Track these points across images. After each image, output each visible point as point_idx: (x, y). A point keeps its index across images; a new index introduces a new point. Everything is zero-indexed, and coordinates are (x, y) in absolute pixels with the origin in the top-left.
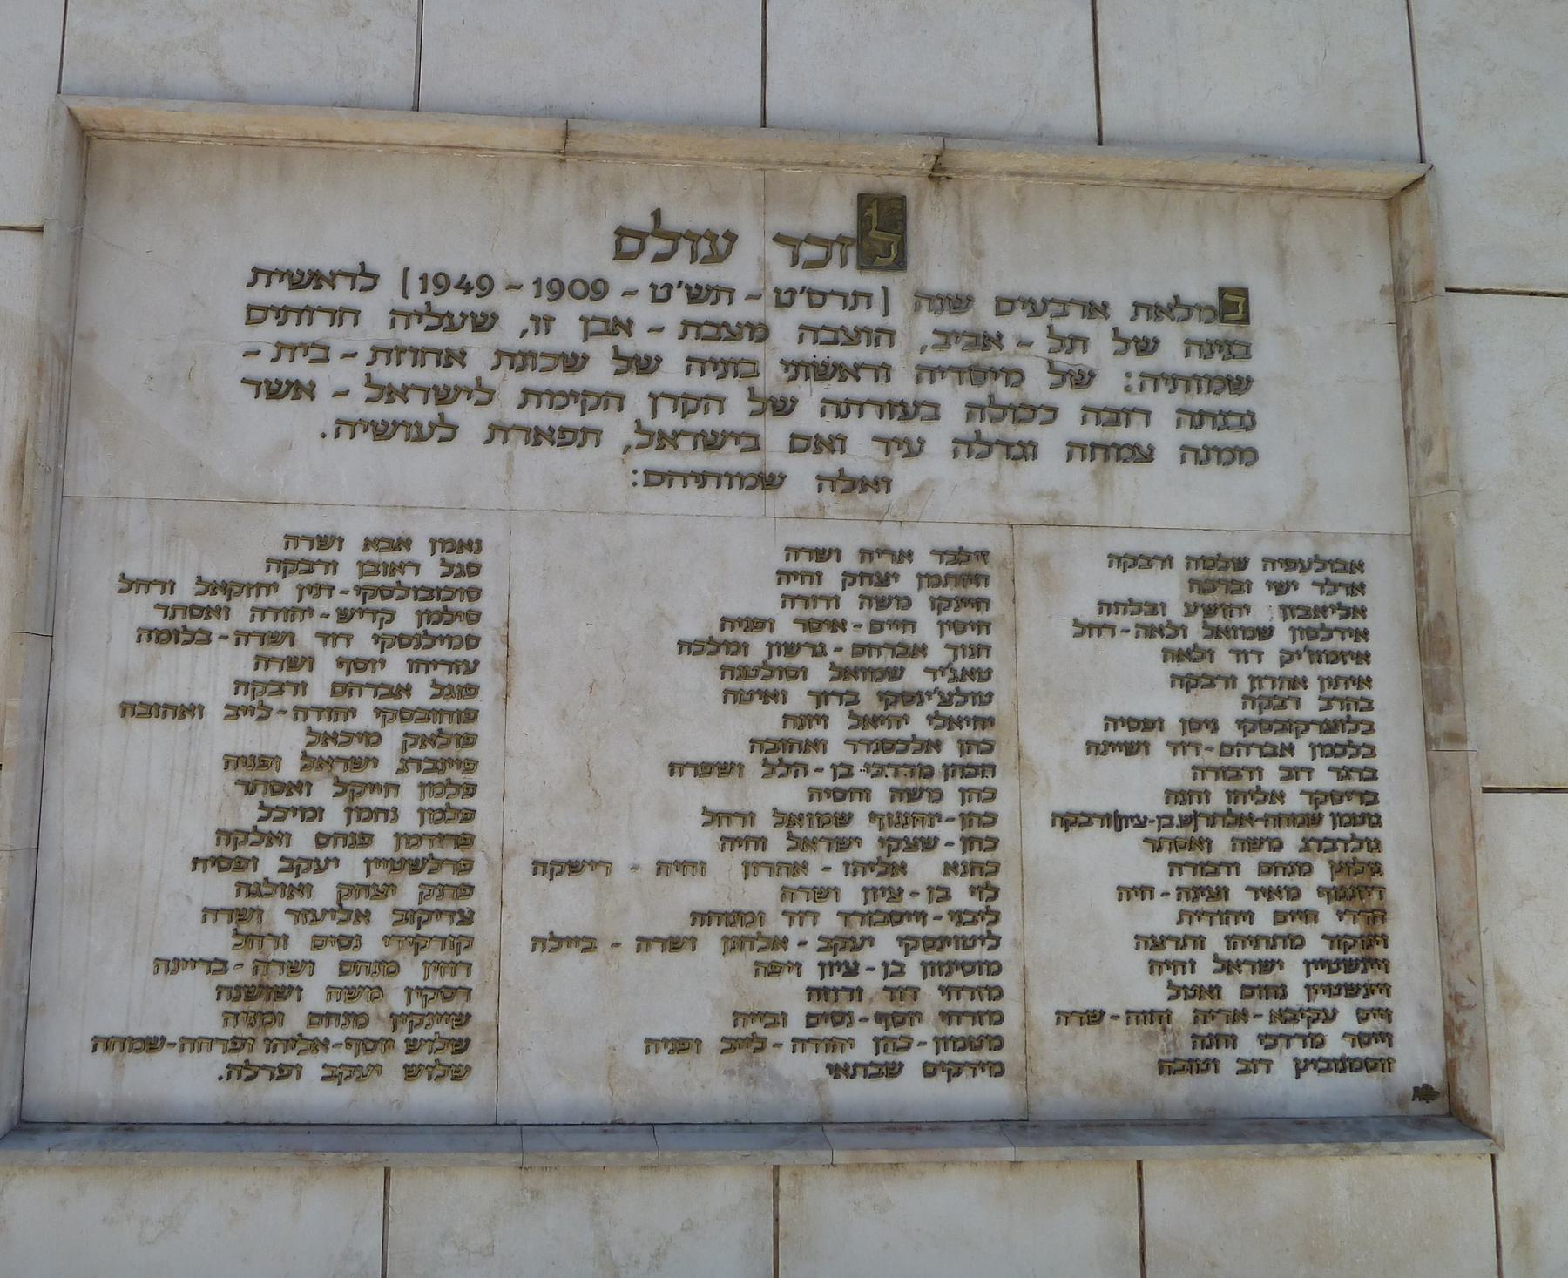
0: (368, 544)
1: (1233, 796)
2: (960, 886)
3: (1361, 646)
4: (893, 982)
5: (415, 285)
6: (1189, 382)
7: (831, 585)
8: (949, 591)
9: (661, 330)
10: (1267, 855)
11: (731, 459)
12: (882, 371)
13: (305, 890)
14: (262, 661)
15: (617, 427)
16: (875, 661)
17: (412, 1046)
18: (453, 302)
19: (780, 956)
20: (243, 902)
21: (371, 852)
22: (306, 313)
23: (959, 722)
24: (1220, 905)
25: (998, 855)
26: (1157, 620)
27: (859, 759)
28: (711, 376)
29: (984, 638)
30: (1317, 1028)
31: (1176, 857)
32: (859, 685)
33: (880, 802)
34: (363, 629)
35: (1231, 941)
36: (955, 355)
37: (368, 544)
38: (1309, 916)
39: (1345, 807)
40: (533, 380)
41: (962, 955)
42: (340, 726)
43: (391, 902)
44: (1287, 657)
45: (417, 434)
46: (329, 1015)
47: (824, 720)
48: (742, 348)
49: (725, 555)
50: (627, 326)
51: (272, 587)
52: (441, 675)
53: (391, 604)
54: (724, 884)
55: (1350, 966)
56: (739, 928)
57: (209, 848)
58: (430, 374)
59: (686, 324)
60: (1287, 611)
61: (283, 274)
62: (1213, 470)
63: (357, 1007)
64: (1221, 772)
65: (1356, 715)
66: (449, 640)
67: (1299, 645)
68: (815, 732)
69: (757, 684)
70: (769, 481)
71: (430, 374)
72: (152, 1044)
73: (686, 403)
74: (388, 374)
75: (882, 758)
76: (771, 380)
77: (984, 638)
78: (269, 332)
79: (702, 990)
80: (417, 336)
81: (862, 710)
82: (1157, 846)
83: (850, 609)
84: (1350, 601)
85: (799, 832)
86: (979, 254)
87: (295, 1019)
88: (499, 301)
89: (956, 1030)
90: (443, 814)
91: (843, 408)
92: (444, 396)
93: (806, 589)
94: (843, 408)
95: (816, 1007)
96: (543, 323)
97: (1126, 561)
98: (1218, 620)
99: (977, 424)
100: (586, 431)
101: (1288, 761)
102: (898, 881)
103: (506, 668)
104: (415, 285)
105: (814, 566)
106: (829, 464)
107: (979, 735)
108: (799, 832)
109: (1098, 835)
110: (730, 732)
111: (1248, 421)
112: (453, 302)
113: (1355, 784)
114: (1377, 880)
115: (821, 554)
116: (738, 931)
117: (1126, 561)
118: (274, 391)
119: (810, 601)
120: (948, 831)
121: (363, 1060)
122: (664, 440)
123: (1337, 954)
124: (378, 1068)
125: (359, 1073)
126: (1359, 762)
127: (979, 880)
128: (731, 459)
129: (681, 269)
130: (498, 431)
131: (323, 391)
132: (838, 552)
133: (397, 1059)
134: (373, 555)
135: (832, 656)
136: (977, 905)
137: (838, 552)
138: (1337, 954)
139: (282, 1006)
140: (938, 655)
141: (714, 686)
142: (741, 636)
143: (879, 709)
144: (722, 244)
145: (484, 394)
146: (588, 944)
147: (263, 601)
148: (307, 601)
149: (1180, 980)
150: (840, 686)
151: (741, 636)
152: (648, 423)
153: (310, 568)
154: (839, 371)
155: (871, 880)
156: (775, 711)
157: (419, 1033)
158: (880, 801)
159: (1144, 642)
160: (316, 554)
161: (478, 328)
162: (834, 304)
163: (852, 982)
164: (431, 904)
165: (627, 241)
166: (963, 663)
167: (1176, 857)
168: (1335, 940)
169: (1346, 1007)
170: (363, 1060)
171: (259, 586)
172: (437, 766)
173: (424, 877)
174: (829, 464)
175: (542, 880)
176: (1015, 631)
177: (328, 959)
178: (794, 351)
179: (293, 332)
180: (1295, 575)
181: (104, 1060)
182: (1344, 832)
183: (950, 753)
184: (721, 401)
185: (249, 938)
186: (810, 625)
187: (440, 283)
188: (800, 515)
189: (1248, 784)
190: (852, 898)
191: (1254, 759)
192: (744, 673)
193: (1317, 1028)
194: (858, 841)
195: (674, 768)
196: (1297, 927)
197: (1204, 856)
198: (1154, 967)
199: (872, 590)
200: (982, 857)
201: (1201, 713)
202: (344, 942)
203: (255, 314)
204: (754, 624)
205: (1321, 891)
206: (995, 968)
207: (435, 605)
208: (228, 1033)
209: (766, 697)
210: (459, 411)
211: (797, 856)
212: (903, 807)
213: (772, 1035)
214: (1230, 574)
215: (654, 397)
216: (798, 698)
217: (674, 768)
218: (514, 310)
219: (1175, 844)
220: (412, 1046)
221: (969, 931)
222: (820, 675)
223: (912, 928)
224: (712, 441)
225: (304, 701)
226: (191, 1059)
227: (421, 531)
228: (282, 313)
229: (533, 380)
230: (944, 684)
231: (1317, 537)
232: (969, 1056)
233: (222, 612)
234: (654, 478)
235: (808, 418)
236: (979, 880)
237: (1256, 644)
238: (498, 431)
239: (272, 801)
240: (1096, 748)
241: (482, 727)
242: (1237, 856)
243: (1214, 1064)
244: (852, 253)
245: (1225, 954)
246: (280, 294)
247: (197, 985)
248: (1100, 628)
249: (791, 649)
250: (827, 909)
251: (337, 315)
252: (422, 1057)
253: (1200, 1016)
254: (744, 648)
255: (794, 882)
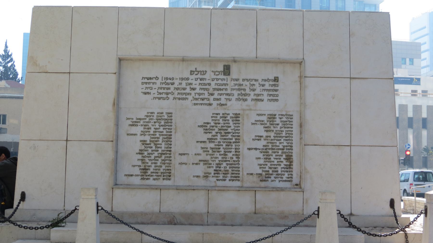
0: (158, 113)
1: (272, 146)
2: (234, 157)
3: (292, 126)
4: (225, 169)
5: (163, 79)
6: (269, 90)
7: (218, 118)
8: (234, 119)
9: (196, 84)
10: (277, 154)
11: (205, 102)
12: (226, 89)
13: (150, 157)
14: (144, 128)
15: (190, 98)
16: (224, 128)
17: (164, 176)
18: (169, 81)
19: (211, 166)
20: (143, 158)
21: (158, 152)
22: (149, 83)
23: (235, 136)
24: (270, 160)
25: (240, 153)
26: (263, 123)
27: (222, 141)
28: (203, 90)
29: (239, 125)
30: (282, 176)
31: (264, 154)
32: (222, 131)
33: (224, 146)
34: (157, 124)
35: (271, 165)
36: (237, 87)
37: (158, 113)
38: (282, 162)
39: (288, 148)
40: (179, 91)
41: (235, 166)
42: (154, 136)
43: (161, 158)
44: (281, 128)
45: (164, 99)
46: (153, 172)
47: (217, 136)
48: (207, 87)
49: (205, 114)
50: (192, 84)
51: (146, 119)
52: (167, 130)
53: (161, 121)
54: (204, 156)
55: (287, 168)
56: (205, 162)
57: (138, 152)
58: (165, 91)
59: (200, 83)
60: (281, 121)
61: (146, 78)
62: (272, 102)
63: (157, 171)
64: (271, 143)
65: (290, 135)
66: (168, 126)
67: (283, 126)
68: (216, 137)
69: (208, 131)
70: (210, 105)
71: (165, 91)
72: (132, 175)
73: (199, 94)
74: (160, 91)
75: (225, 141)
76: (211, 91)
77: (239, 125)
78: (145, 86)
79: (200, 170)
80: (164, 86)
81: (222, 135)
82: (261, 152)
83: (221, 121)
84: (290, 120)
85: (213, 150)
86: (240, 73)
87: (149, 172)
88: (175, 81)
89: (233, 175)
90: (167, 148)
91: (221, 95)
92: (167, 94)
93: (215, 119)
94: (221, 95)
95: (215, 172)
96: (180, 84)
97: (258, 115)
98: (271, 123)
99: (239, 96)
100: (186, 98)
101: (280, 141)
102: (227, 156)
103: (176, 129)
104: (163, 79)
105: (216, 116)
106: (218, 102)
107: (238, 138)
108: (213, 150)
109: (253, 151)
110: (205, 137)
111: (277, 96)
112: (169, 81)
113: (290, 145)
114: (292, 157)
115: (217, 114)
116: (205, 162)
117: (258, 115)
118: (145, 93)
119: (215, 120)
120: (233, 150)
121: (158, 178)
122: (196, 99)
123: (286, 167)
124: (160, 179)
125: (157, 179)
126: (290, 142)
127: (237, 156)
128: (205, 102)
129: (199, 76)
130: (174, 98)
131: (152, 93)
132: (219, 114)
133: (161, 178)
134: (158, 115)
135: (218, 127)
136: (237, 160)
137: (219, 114)
138: (286, 167)
139: (147, 171)
140: (233, 127)
141: (203, 131)
142: (206, 125)
143: (224, 134)
144: (205, 72)
145: (173, 93)
146: (186, 164)
147: (144, 121)
148: (150, 121)
149: (264, 170)
150: (219, 131)
151: (206, 125)
152: (194, 97)
153: (150, 116)
154: (220, 89)
155: (223, 156)
156: (211, 135)
157: (165, 174)
158: (224, 146)
159: (261, 126)
160: (151, 115)
161: (172, 84)
162: (220, 80)
163: (220, 169)
164: (166, 159)
165: (192, 73)
166: (236, 128)
167: (264, 154)
168: (285, 165)
169: (286, 174)
170: (158, 178)
171: (144, 119)
172: (167, 141)
173: (165, 155)
174: (218, 102)
175: (180, 156)
176: (243, 124)
177: (153, 165)
178: (214, 87)
179: (148, 86)
180: (283, 117)
181: (126, 177)
182: (288, 151)
183: (234, 140)
184: (204, 94)
185: (143, 163)
186: (215, 123)
187: (167, 79)
188: (215, 109)
189: (275, 144)
190: (220, 158)
191: (276, 141)
192: (207, 130)
193: (282, 176)
194: (221, 151)
195: (197, 142)
196: (280, 163)
197: (268, 154)
198: (260, 168)
199: (224, 119)
200: (237, 153)
201: (268, 135)
202: (155, 163)
203: (143, 83)
204: (208, 123)
205: (284, 159)
206: (239, 168)
207: (166, 121)
208: (141, 174)
209: (209, 133)
210: (170, 96)
211: (213, 153)
212: (227, 147)
213: (209, 176)
214: (274, 117)
215: (195, 93)
216: (214, 133)
217: (197, 142)
218: (177, 82)
219: (264, 152)
220: (164, 176)
221: (235, 163)
222: (217, 130)
223: (228, 162)
224: (203, 99)
225: (150, 133)
226: (136, 177)
227: (165, 111)
228: (146, 83)
229: (179, 91)
230: (233, 131)
231: (286, 111)
232: (235, 179)
233: (139, 122)
234: (195, 104)
235: (216, 96)
236: (237, 156)
237: (277, 126)
238: (174, 98)
239: (146, 146)
240: (253, 139)
241: (172, 137)
242: (272, 154)
243: (268, 180)
244: (223, 73)
245: (270, 166)
246: (146, 81)
247: (137, 168)
248: (255, 124)
249: (213, 126)
250: (217, 160)
251: (153, 83)
252: (165, 177)
253: (266, 174)
254: (207, 126)
255: (212, 156)
